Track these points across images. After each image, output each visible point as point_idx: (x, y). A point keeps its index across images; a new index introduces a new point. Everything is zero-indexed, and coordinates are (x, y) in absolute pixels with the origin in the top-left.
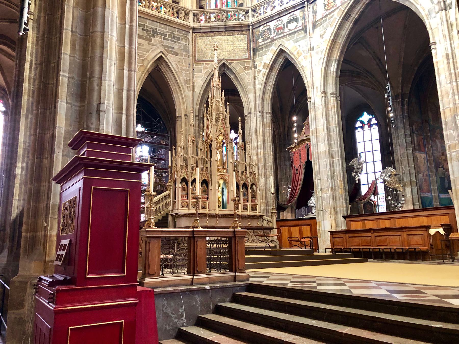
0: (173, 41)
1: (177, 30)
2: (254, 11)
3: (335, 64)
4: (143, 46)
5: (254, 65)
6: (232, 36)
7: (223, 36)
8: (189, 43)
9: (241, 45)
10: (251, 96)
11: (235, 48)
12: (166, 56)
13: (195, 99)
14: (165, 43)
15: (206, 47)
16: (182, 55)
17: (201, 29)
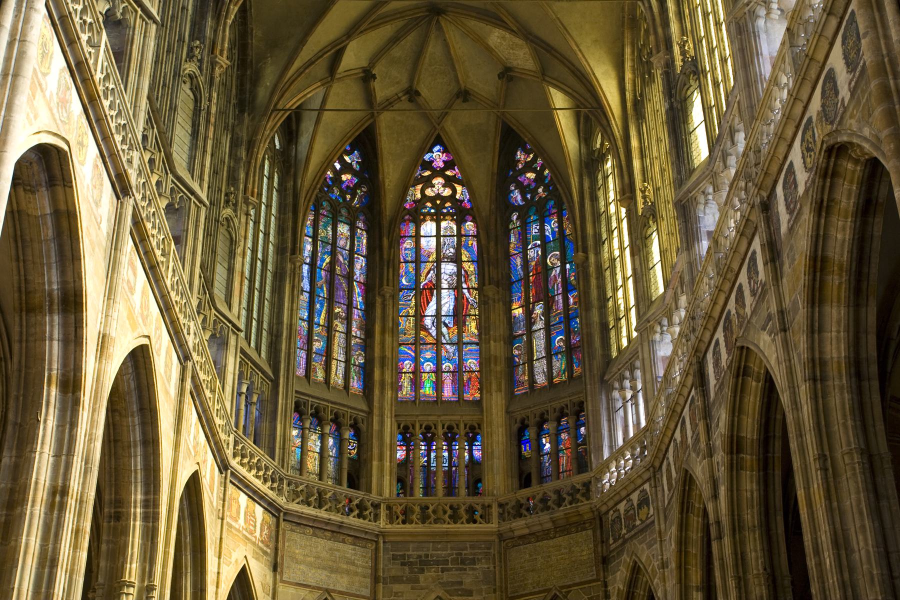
0: (461, 569)
4: (402, 596)
7: (551, 538)
9: (584, 553)
11: (573, 559)
14: (446, 577)
16: (480, 592)
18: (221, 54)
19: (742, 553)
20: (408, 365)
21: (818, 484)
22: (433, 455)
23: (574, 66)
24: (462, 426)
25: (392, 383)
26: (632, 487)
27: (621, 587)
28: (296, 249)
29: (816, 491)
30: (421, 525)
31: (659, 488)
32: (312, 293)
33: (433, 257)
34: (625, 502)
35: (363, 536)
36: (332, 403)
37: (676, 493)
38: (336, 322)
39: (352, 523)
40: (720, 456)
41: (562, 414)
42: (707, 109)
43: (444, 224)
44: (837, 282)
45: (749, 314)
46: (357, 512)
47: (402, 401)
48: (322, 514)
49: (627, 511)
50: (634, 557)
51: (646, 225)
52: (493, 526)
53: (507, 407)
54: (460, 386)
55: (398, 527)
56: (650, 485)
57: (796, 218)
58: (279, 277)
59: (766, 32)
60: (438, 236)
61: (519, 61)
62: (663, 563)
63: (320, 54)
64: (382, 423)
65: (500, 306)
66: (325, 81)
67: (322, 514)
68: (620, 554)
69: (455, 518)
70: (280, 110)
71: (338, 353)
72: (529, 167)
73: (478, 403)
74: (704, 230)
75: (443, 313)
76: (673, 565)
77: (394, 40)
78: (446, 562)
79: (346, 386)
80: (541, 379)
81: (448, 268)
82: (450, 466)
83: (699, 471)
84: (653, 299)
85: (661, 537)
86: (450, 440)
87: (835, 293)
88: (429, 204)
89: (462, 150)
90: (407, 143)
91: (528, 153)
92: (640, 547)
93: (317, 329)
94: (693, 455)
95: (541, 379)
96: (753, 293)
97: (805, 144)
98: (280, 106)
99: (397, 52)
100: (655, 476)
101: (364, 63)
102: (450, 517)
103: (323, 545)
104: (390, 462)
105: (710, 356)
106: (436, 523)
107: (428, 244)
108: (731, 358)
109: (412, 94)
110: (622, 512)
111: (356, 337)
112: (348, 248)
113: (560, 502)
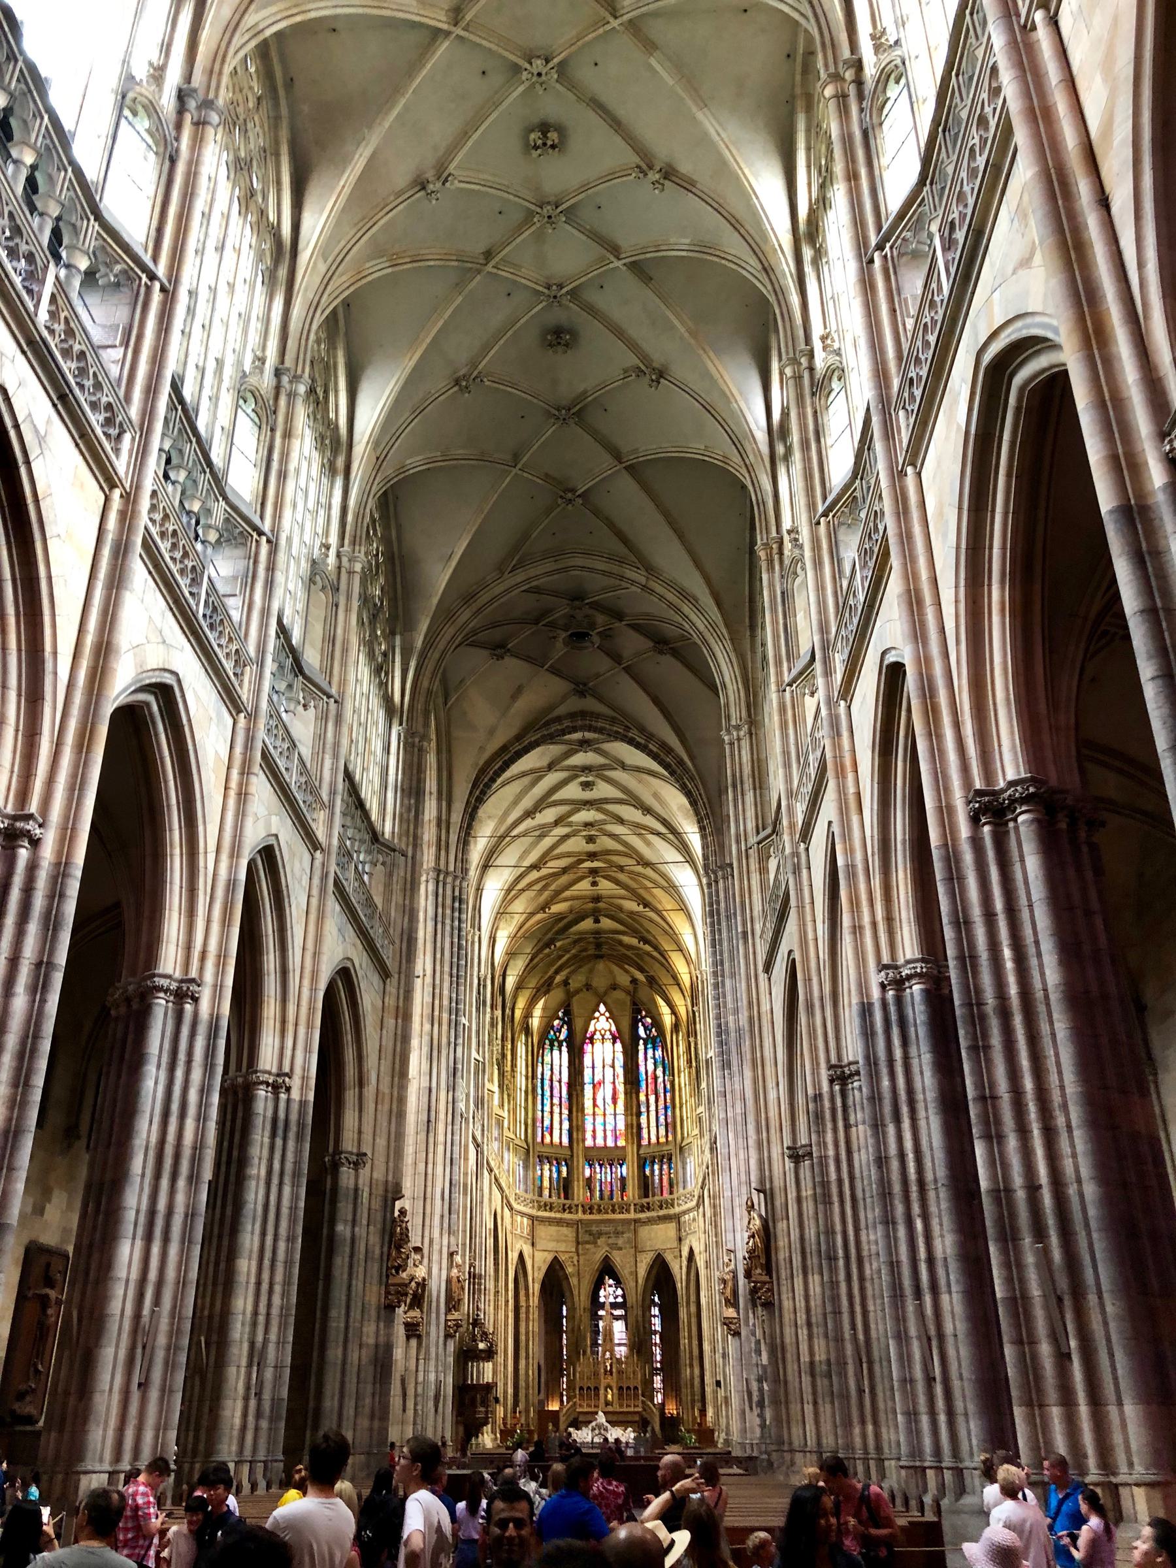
14: (611, 1241)
20: (589, 1127)
32: (543, 1095)
41: (663, 1157)
48: (552, 1215)
52: (632, 1215)
54: (616, 1138)
55: (588, 1217)
58: (526, 1092)
65: (634, 1096)
67: (552, 1215)
69: (613, 1211)
73: (623, 1148)
80: (654, 1139)
81: (609, 1072)
86: (611, 1165)
89: (614, 1010)
95: (654, 1139)
103: (553, 1230)
109: (588, 987)
113: (661, 1207)
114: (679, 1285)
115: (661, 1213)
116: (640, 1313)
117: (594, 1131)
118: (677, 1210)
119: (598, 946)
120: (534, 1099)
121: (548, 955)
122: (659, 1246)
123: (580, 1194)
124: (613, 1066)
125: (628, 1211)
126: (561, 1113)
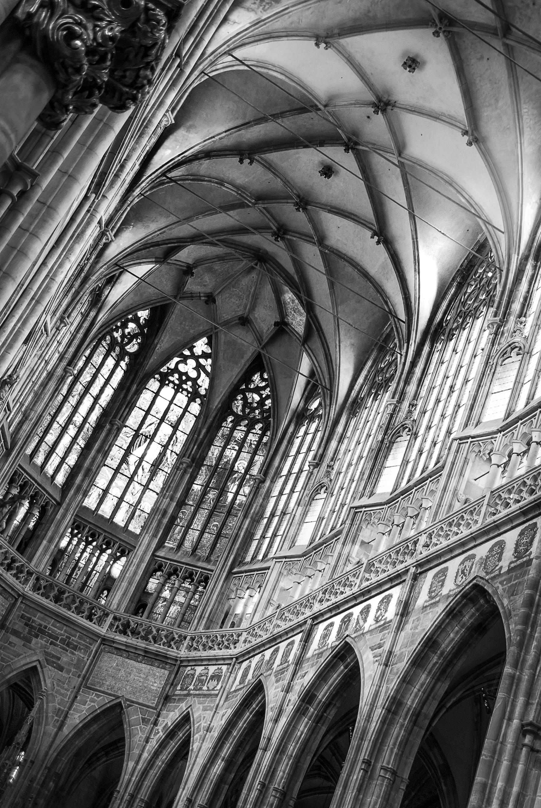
0: (64, 649)
1: (78, 634)
2: (193, 639)
3: (221, 763)
5: (156, 720)
6: (149, 667)
7: (138, 661)
8: (89, 656)
9: (156, 685)
10: (131, 764)
11: (146, 685)
12: (42, 668)
13: (57, 742)
14: (51, 649)
15: (110, 670)
16: (68, 672)
17: (114, 642)
18: (112, 230)
19: (274, 769)
21: (357, 778)
22: (86, 555)
23: (329, 351)
24: (117, 546)
25: (86, 490)
26: (214, 663)
27: (169, 724)
28: (72, 362)
29: (354, 781)
30: (53, 603)
31: (233, 675)
33: (160, 416)
34: (203, 667)
35: (10, 591)
36: (38, 484)
37: (245, 689)
38: (71, 427)
39: (8, 578)
40: (294, 697)
42: (405, 462)
43: (179, 394)
44: (435, 661)
45: (366, 630)
46: (15, 572)
47: (85, 507)
49: (201, 675)
50: (189, 709)
51: (317, 491)
52: (103, 630)
53: (156, 550)
56: (228, 669)
57: (432, 604)
58: (50, 375)
59: (474, 462)
60: (171, 402)
61: (294, 322)
62: (209, 727)
63: (167, 242)
64: (64, 516)
66: (158, 260)
68: (180, 700)
69: (79, 611)
70: (119, 266)
71: (61, 450)
72: (257, 390)
74: (360, 538)
75: (146, 459)
76: (215, 734)
77: (221, 258)
78: (56, 639)
79: (53, 477)
80: (188, 545)
81: (166, 430)
82: (93, 569)
83: (273, 693)
84: (296, 544)
85: (216, 709)
87: (430, 666)
88: (176, 376)
89: (221, 354)
90: (187, 328)
91: (262, 379)
92: (198, 706)
93: (55, 425)
94: (273, 678)
96: (377, 620)
97: (462, 567)
98: (119, 263)
99: (217, 266)
100: (234, 665)
101: (190, 261)
102: (76, 608)
104: (55, 547)
105: (322, 627)
106: (64, 607)
107: (161, 405)
108: (337, 643)
109: (210, 299)
110: (197, 673)
111: (78, 444)
112: (106, 377)
114: (131, 764)
115: (154, 647)
116: (40, 777)
117: (106, 492)
118: (183, 653)
119: (282, 232)
120: (57, 390)
121: (221, 182)
122: (125, 692)
123: (40, 561)
124: (175, 427)
125: (100, 622)
126: (74, 439)
